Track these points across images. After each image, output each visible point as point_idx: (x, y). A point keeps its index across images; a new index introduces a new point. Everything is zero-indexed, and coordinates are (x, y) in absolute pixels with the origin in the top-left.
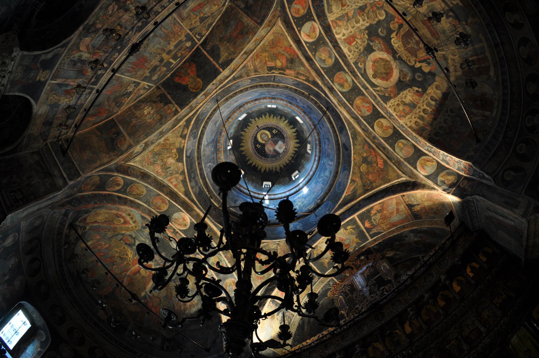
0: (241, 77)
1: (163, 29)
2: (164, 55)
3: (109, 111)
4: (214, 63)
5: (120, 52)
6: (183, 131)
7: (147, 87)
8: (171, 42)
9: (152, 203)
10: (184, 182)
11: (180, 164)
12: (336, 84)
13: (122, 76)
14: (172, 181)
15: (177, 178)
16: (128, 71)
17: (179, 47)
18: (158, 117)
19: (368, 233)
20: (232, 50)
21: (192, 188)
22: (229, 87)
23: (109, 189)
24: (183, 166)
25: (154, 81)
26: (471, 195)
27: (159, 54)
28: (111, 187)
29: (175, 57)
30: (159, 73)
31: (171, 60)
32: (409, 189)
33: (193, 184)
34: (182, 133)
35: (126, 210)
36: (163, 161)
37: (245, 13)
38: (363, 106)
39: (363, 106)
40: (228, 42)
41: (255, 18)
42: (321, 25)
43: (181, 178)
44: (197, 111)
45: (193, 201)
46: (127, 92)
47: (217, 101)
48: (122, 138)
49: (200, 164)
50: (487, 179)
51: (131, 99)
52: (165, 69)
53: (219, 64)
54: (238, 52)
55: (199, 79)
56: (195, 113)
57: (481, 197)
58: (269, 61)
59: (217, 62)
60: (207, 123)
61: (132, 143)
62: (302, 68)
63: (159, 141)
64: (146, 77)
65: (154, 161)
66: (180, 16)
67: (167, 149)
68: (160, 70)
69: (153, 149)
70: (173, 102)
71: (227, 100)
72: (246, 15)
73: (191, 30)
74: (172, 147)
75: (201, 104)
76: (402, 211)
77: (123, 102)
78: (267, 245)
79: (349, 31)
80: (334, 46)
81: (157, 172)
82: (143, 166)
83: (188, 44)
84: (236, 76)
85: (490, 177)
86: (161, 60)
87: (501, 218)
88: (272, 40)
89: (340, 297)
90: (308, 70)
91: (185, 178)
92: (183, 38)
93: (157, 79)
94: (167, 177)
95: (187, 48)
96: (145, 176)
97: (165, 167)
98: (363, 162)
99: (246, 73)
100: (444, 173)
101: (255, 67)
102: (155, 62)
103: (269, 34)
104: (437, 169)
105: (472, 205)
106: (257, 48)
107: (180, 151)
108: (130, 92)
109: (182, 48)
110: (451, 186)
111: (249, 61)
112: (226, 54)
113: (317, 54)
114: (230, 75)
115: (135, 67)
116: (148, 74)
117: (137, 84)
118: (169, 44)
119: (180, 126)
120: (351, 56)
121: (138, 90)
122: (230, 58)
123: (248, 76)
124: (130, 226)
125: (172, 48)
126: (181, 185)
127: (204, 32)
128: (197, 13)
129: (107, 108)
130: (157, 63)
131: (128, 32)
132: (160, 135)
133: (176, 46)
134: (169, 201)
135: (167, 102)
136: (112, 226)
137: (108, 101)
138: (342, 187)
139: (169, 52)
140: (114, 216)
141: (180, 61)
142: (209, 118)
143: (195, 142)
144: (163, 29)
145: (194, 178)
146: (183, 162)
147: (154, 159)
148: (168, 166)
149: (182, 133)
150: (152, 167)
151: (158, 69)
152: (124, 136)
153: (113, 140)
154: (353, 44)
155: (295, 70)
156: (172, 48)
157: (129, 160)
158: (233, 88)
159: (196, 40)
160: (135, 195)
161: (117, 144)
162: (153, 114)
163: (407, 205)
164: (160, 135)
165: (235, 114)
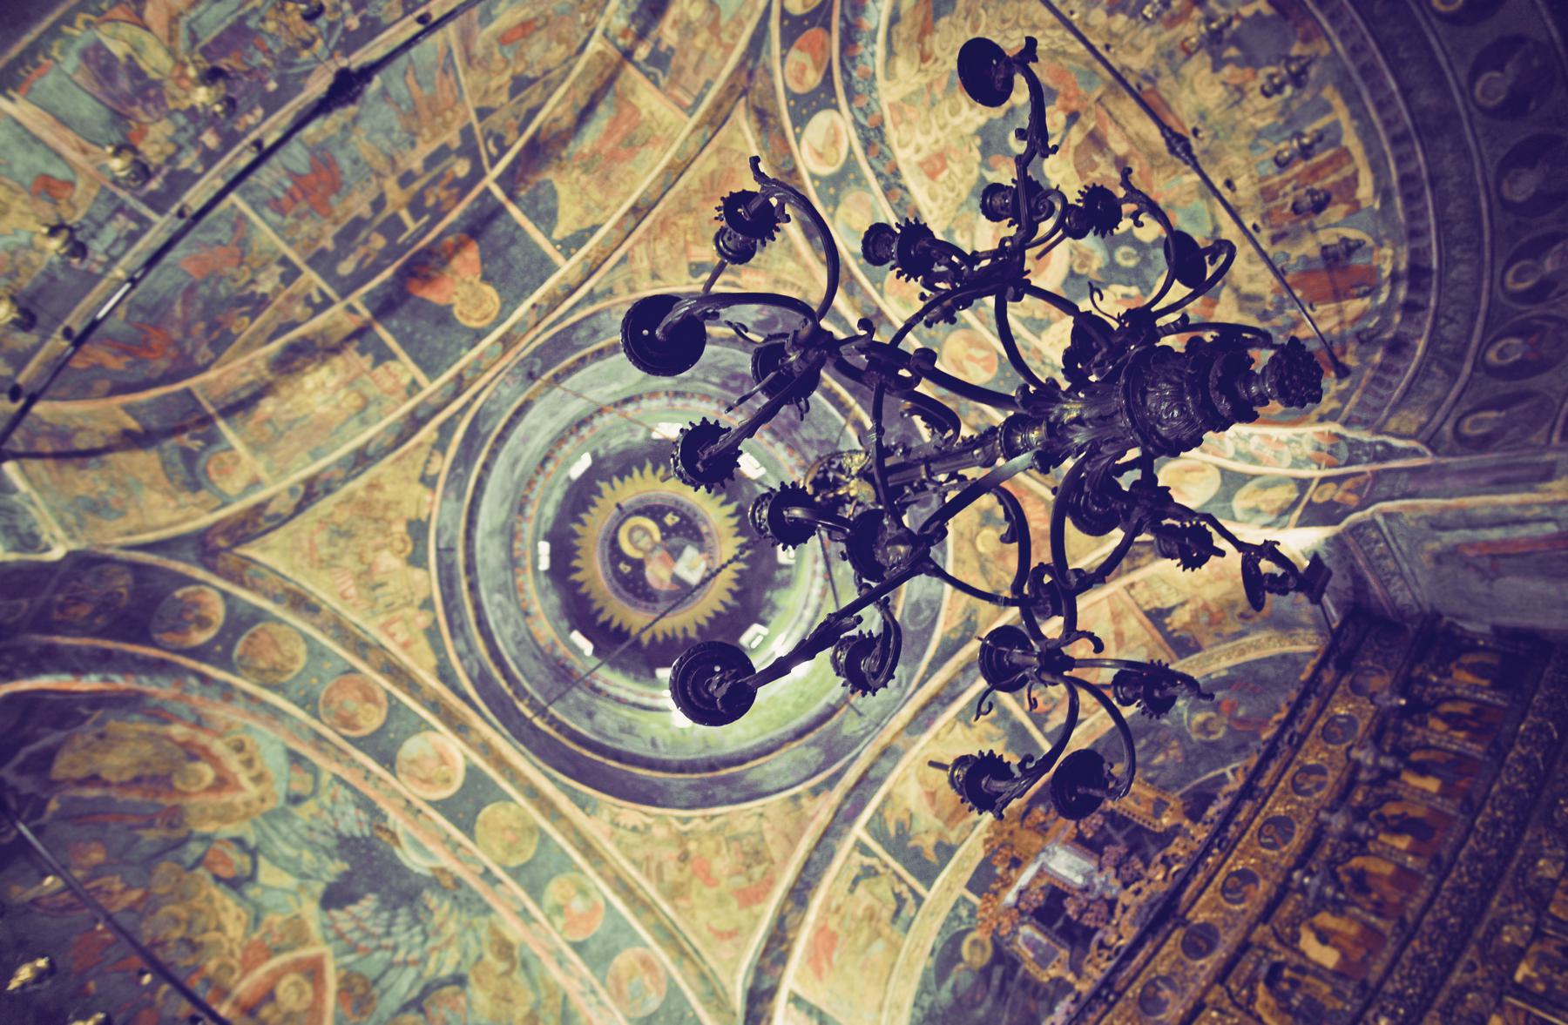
0: (610, 292)
1: (410, 79)
2: (391, 184)
3: (182, 351)
4: (538, 236)
5: (272, 104)
6: (428, 461)
7: (317, 299)
8: (419, 140)
9: (327, 703)
10: (432, 633)
11: (418, 574)
12: (889, 299)
13: (254, 217)
14: (393, 628)
15: (407, 622)
16: (277, 206)
17: (436, 171)
18: (353, 401)
19: (1040, 727)
20: (597, 196)
21: (461, 657)
22: (574, 326)
23: (168, 638)
24: (427, 581)
25: (343, 279)
26: (1362, 507)
27: (379, 175)
28: (173, 629)
29: (416, 207)
30: (361, 251)
31: (405, 215)
32: (1143, 561)
33: (462, 647)
34: (425, 468)
35: (229, 726)
36: (361, 558)
37: (647, 75)
38: (971, 358)
39: (971, 358)
40: (586, 172)
41: (678, 93)
42: (856, 123)
43: (423, 620)
44: (475, 397)
45: (465, 698)
46: (253, 293)
47: (531, 376)
48: (225, 456)
49: (473, 587)
50: (1404, 453)
51: (261, 330)
52: (379, 242)
53: (554, 243)
54: (613, 202)
55: (489, 290)
56: (467, 406)
57: (1399, 503)
58: (696, 243)
59: (548, 235)
60: (494, 453)
61: (264, 475)
62: (791, 265)
63: (351, 486)
64: (322, 253)
65: (333, 557)
66: (466, 37)
67: (376, 520)
68: (366, 241)
69: (331, 515)
70: (402, 354)
71: (557, 379)
72: (648, 85)
73: (483, 113)
74: (391, 515)
75: (489, 376)
76: (1134, 638)
77: (234, 330)
78: (727, 824)
79: (931, 139)
80: (887, 190)
81: (343, 597)
82: (294, 569)
83: (462, 168)
84: (597, 290)
85: (1412, 444)
86: (378, 204)
87: (1496, 534)
88: (713, 173)
89: (1026, 930)
90: (806, 267)
91: (436, 621)
92: (453, 138)
93: (352, 276)
94: (374, 614)
95: (456, 182)
96: (301, 602)
97: (368, 580)
98: (982, 525)
99: (627, 282)
100: (1251, 485)
101: (652, 260)
102: (359, 204)
103: (708, 150)
104: (1224, 483)
105: (1374, 535)
106: (668, 197)
107: (418, 529)
108: (264, 296)
109: (441, 176)
110: (1284, 512)
111: (638, 242)
112: (578, 210)
113: (841, 210)
114: (582, 283)
115: (298, 195)
116: (328, 244)
117: (291, 274)
118: (413, 145)
119: (419, 445)
120: (936, 213)
121: (291, 298)
122: (587, 224)
123: (632, 290)
124: (238, 799)
125: (417, 165)
126: (423, 644)
127: (510, 137)
128: (510, 56)
129: (176, 334)
130: (364, 210)
131: (314, 39)
132: (356, 464)
133: (431, 161)
134: (388, 693)
135: (383, 356)
136: (163, 800)
137: (185, 303)
138: (927, 613)
139: (406, 179)
140: (180, 753)
141: (429, 227)
142: (502, 438)
143: (459, 511)
144: (410, 79)
145: (462, 627)
146: (427, 568)
147: (333, 550)
148: (378, 578)
149: (425, 468)
150: (324, 577)
151: (363, 235)
152: (231, 449)
153: (189, 457)
154: (943, 176)
155: (768, 271)
156: (417, 165)
157: (246, 539)
158: (582, 333)
159: (485, 162)
160: (262, 671)
161: (206, 472)
162: (336, 389)
163: (1148, 614)
164: (356, 464)
165: (566, 448)
